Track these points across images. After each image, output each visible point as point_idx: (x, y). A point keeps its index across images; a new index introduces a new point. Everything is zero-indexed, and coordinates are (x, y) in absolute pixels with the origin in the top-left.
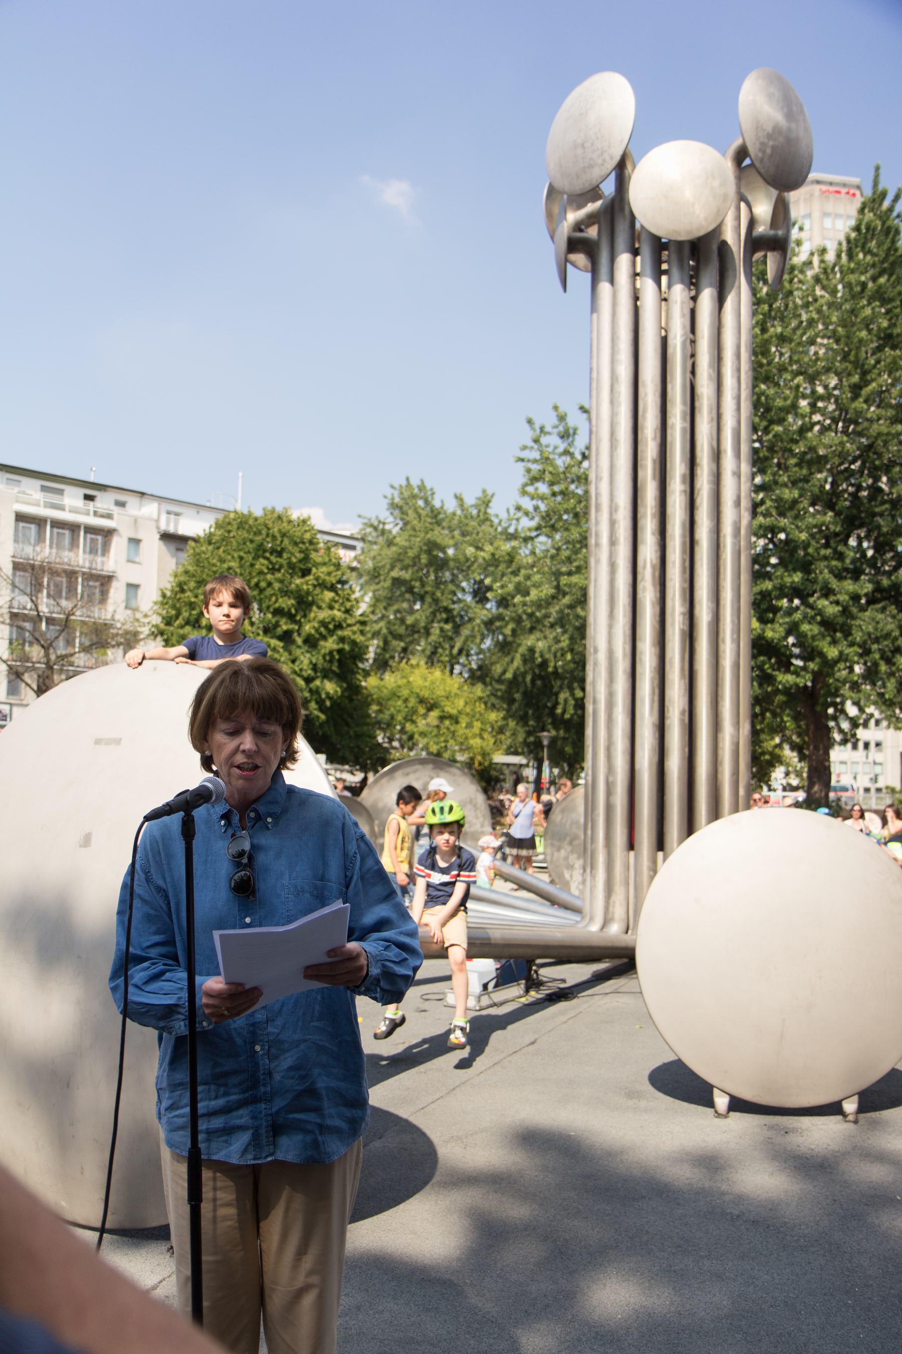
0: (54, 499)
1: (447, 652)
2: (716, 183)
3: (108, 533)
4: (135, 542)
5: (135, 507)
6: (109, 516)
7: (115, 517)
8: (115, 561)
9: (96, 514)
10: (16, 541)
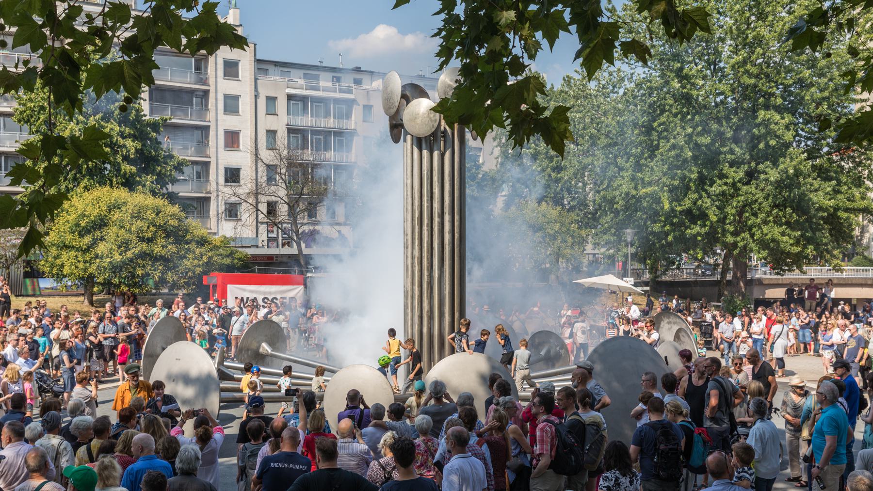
0: (313, 83)
4: (368, 108)
6: (350, 91)
8: (355, 121)
9: (341, 91)
10: (289, 113)
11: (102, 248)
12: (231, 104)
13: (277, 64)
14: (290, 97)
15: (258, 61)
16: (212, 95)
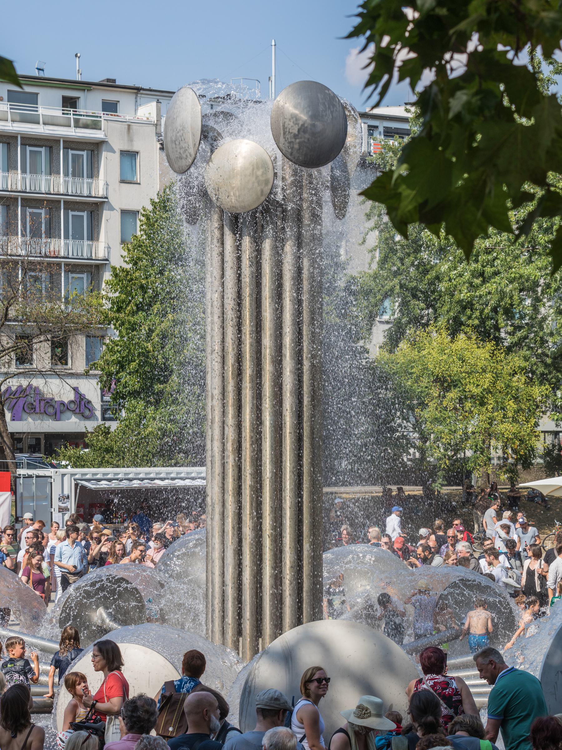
0: (25, 109)
1: (477, 313)
2: (259, 173)
3: (95, 148)
6: (96, 126)
7: (103, 124)
8: (105, 181)
9: (78, 124)
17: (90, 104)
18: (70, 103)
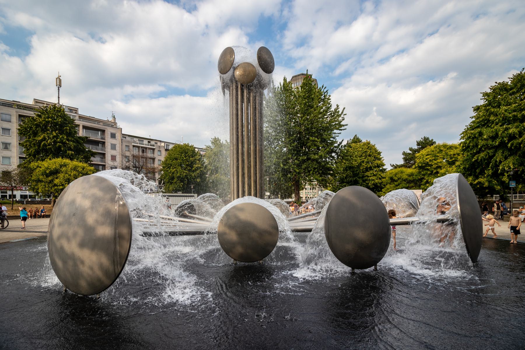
3: (154, 149)
5: (159, 144)
11: (56, 181)
12: (113, 147)
13: (129, 136)
14: (134, 146)
15: (123, 134)
16: (106, 143)
17: (153, 143)
18: (149, 142)
